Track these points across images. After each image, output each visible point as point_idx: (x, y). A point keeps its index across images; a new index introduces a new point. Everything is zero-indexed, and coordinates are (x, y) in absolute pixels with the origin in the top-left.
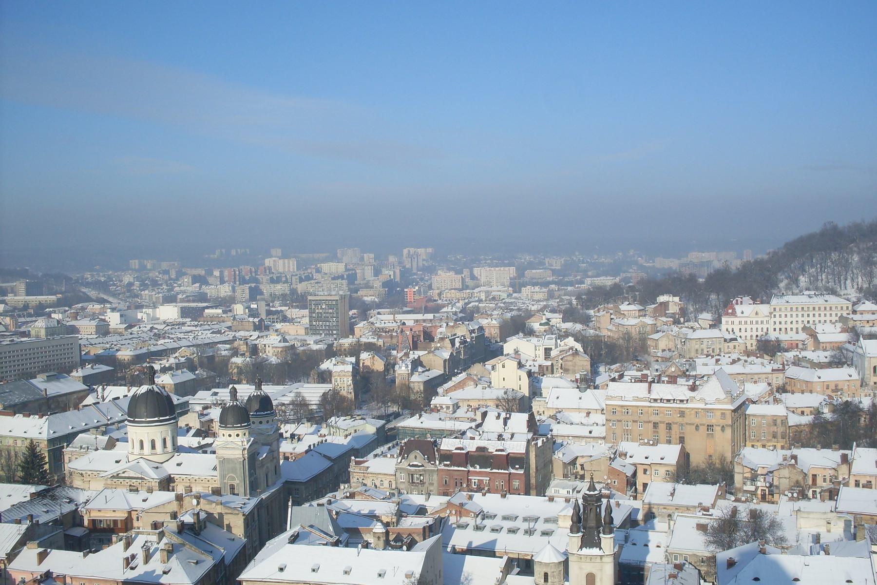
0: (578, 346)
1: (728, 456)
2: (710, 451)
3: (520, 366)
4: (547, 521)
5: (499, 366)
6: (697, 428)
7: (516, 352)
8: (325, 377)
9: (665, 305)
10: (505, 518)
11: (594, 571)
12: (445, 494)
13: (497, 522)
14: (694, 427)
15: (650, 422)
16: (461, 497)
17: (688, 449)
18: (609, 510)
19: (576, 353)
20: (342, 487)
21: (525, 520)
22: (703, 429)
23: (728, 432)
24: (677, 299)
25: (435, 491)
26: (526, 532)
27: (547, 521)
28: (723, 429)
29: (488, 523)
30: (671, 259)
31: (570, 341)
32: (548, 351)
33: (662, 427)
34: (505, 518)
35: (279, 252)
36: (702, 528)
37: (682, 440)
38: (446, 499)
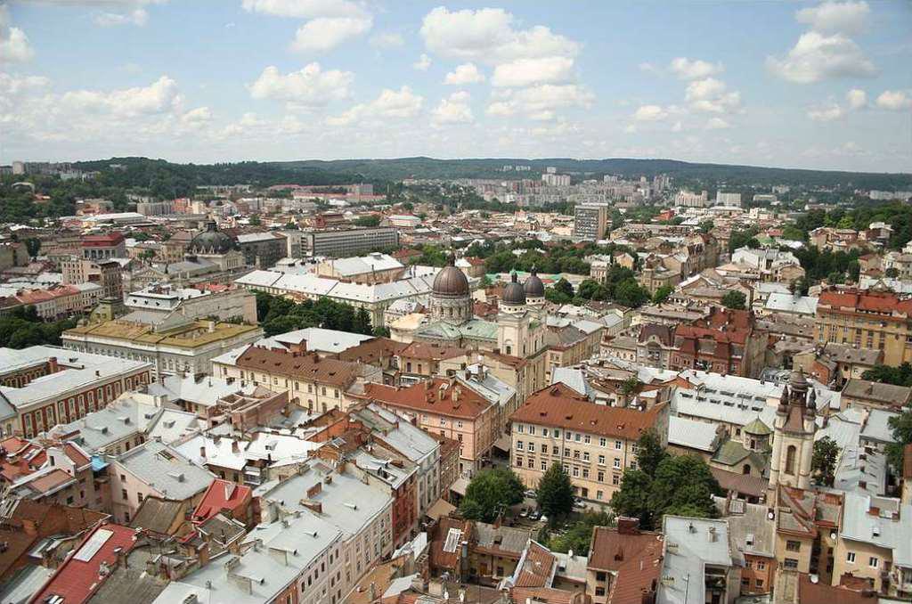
0: (797, 261)
4: (757, 399)
6: (897, 337)
7: (742, 261)
8: (586, 270)
9: (877, 231)
10: (723, 393)
11: (795, 445)
12: (675, 369)
13: (716, 397)
14: (894, 337)
15: (854, 328)
17: (886, 352)
18: (813, 397)
19: (794, 266)
20: (594, 356)
21: (740, 396)
24: (888, 227)
25: (667, 367)
26: (739, 406)
27: (757, 399)
29: (709, 396)
30: (886, 192)
31: (790, 254)
32: (769, 262)
34: (723, 393)
35: (554, 170)
37: (882, 346)
38: (675, 373)
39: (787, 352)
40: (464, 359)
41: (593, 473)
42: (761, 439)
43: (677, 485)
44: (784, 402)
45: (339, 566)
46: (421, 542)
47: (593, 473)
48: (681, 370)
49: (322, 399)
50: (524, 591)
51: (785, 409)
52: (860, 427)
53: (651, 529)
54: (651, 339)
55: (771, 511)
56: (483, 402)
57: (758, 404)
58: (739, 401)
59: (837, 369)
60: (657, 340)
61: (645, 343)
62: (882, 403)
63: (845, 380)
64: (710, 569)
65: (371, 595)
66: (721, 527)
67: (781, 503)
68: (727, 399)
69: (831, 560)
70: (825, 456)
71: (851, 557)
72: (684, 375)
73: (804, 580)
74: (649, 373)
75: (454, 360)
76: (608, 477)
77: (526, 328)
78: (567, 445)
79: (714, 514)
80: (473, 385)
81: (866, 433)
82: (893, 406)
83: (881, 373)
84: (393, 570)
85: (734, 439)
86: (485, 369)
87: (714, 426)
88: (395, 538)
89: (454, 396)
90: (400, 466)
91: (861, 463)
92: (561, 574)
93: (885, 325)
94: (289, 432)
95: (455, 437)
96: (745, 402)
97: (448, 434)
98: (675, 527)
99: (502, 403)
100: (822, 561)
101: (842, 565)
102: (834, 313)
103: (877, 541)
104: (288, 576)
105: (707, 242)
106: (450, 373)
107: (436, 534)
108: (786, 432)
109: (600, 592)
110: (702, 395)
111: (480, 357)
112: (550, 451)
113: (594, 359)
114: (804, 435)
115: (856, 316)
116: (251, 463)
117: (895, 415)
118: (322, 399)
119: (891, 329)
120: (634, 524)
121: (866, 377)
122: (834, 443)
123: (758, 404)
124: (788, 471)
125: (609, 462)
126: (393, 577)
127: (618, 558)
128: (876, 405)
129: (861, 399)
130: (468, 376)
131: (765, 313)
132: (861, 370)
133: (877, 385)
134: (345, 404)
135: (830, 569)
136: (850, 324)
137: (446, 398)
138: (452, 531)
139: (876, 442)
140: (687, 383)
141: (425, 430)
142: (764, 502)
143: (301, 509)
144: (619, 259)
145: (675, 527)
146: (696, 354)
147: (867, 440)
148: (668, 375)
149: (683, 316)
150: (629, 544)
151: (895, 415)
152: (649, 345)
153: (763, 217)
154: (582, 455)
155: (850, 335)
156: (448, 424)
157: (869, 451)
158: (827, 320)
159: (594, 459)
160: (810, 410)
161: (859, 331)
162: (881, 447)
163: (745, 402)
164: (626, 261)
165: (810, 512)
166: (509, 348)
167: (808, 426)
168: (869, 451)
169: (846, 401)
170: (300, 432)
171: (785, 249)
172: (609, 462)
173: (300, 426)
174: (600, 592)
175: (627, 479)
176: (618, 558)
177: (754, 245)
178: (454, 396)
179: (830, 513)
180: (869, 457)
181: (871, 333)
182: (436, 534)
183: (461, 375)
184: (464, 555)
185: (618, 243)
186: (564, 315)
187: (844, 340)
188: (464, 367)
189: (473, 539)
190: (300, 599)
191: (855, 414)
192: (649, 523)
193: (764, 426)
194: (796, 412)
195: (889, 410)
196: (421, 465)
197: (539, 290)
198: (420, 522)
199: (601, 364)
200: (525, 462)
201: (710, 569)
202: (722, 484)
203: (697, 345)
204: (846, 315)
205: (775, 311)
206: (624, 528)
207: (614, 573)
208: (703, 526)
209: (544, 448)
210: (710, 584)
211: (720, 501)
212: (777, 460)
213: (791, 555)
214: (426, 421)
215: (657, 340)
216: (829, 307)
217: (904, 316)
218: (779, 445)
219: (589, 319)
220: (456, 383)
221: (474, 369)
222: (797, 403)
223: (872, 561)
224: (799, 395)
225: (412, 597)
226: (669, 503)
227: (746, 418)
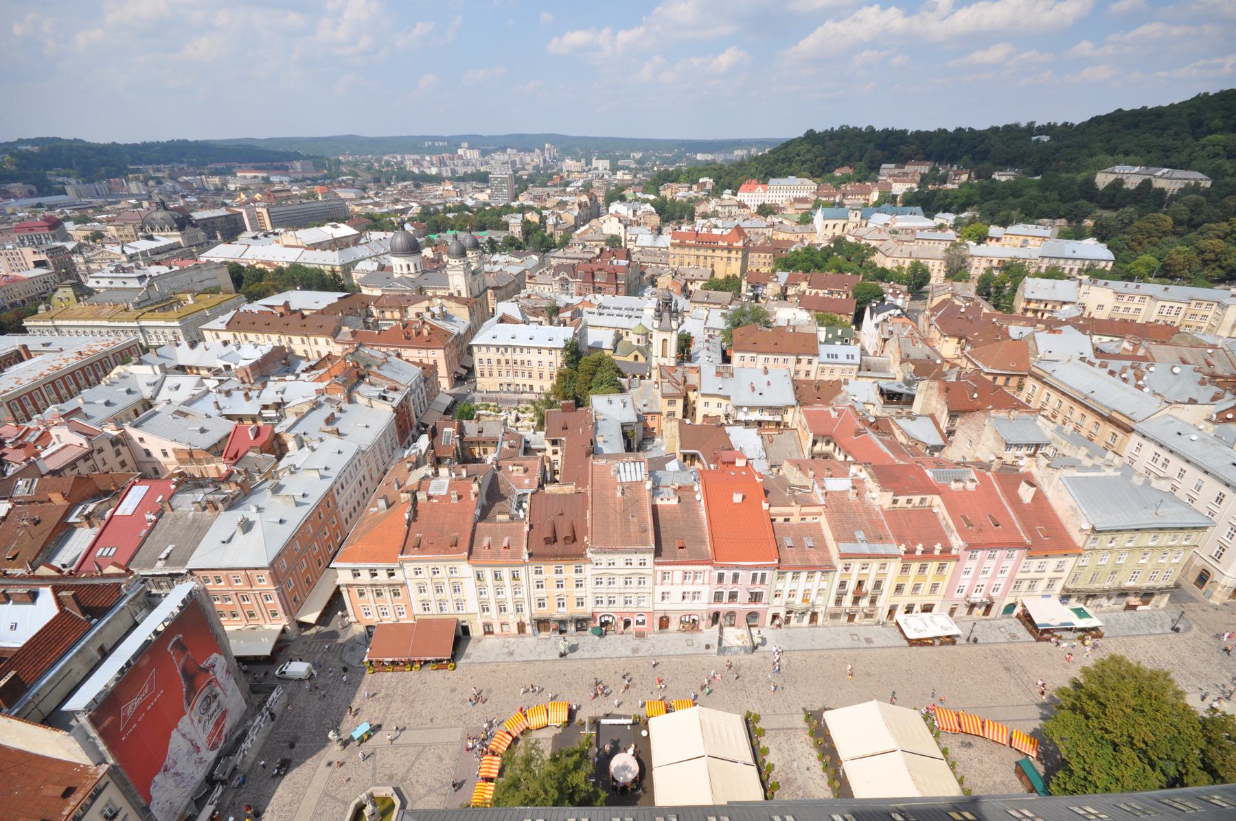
1: (738, 275)
2: (728, 273)
3: (620, 221)
5: (607, 221)
8: (506, 226)
10: (614, 308)
12: (580, 295)
13: (611, 311)
16: (590, 297)
18: (676, 305)
19: (651, 213)
22: (725, 260)
23: (740, 261)
24: (711, 181)
28: (736, 259)
29: (605, 311)
32: (635, 211)
33: (702, 258)
36: (723, 314)
37: (712, 266)
38: (582, 298)
39: (653, 275)
40: (426, 303)
41: (536, 374)
42: (647, 335)
43: (593, 374)
44: (657, 310)
45: (364, 470)
46: (424, 442)
47: (536, 374)
48: (585, 296)
49: (315, 348)
50: (506, 462)
51: (659, 315)
52: (703, 322)
53: (582, 406)
54: (561, 275)
55: (656, 383)
56: (447, 334)
57: (639, 313)
58: (626, 313)
59: (686, 284)
60: (566, 276)
61: (557, 278)
62: (715, 304)
63: (691, 292)
64: (623, 426)
65: (396, 486)
66: (626, 397)
67: (662, 377)
68: (617, 312)
69: (694, 409)
70: (685, 343)
71: (706, 404)
72: (587, 299)
73: (681, 423)
74: (563, 300)
75: (419, 305)
76: (546, 375)
77: (470, 275)
78: (515, 358)
79: (622, 390)
80: (440, 323)
81: (708, 325)
82: (724, 307)
83: (714, 285)
84: (409, 466)
85: (625, 339)
86: (444, 309)
87: (612, 331)
88: (402, 441)
89: (425, 332)
90: (396, 390)
91: (706, 345)
92: (528, 446)
93: (714, 251)
94: (293, 378)
95: (432, 363)
96: (630, 313)
97: (425, 361)
98: (599, 403)
99: (462, 332)
100: (688, 410)
101: (701, 411)
102: (682, 245)
103: (721, 393)
104: (327, 484)
105: (591, 200)
106: (418, 315)
107: (434, 434)
108: (661, 329)
109: (555, 453)
110: (601, 311)
111: (439, 301)
112: (503, 362)
113: (523, 293)
114: (672, 330)
115: (697, 247)
116: (266, 407)
117: (724, 311)
118: (315, 348)
119: (718, 253)
120: (572, 404)
121: (705, 288)
122: (689, 334)
123: (639, 313)
124: (664, 356)
125: (545, 364)
126: (410, 470)
127: (565, 428)
128: (712, 306)
129: (702, 303)
130: (433, 316)
131: (636, 249)
132: (701, 283)
133: (712, 292)
134: (337, 350)
135: (694, 414)
136: (693, 251)
137: (419, 333)
138: (446, 430)
139: (714, 330)
140: (590, 304)
141: (407, 360)
142: (650, 377)
143: (323, 435)
144: (529, 216)
145: (599, 403)
146: (594, 283)
147: (709, 329)
148: (576, 300)
149: (581, 256)
150: (571, 417)
151: (724, 311)
152: (561, 279)
153: (627, 177)
154: (526, 363)
155: (693, 260)
156: (424, 352)
157: (710, 336)
158: (678, 250)
159: (535, 364)
160: (676, 314)
161: (698, 256)
162: (717, 333)
163: (630, 313)
164: (533, 217)
165: (680, 380)
166: (459, 292)
167: (674, 324)
168: (710, 336)
169: (693, 305)
170: (304, 376)
171: (646, 201)
172: (545, 364)
173: (303, 371)
174: (555, 453)
175: (560, 374)
176: (565, 428)
177: (623, 199)
178: (425, 332)
179: (693, 379)
180: (711, 340)
181: (705, 258)
182: (434, 434)
183: (427, 316)
184: (458, 445)
185: (526, 203)
186: (495, 263)
187: (689, 264)
188: (428, 309)
189: (461, 431)
190: (337, 500)
191: (702, 311)
192: (579, 403)
193: (645, 328)
194: (666, 315)
195: (722, 308)
196: (411, 386)
197: (476, 246)
198: (418, 428)
199: (529, 297)
200: (486, 373)
201: (623, 426)
202: (623, 370)
203: (593, 276)
204: (690, 246)
205: (643, 247)
206: (565, 409)
207: (563, 439)
208: (617, 398)
209: (499, 361)
210: (625, 435)
211: (624, 381)
212: (656, 349)
213: (671, 409)
214: (406, 353)
215: (566, 276)
216: (678, 241)
217: (726, 244)
218: (657, 339)
219: (517, 264)
220: (424, 323)
221: (436, 310)
222: (666, 309)
223: (719, 405)
224: (667, 304)
225: (427, 482)
226: (590, 388)
227: (633, 324)
